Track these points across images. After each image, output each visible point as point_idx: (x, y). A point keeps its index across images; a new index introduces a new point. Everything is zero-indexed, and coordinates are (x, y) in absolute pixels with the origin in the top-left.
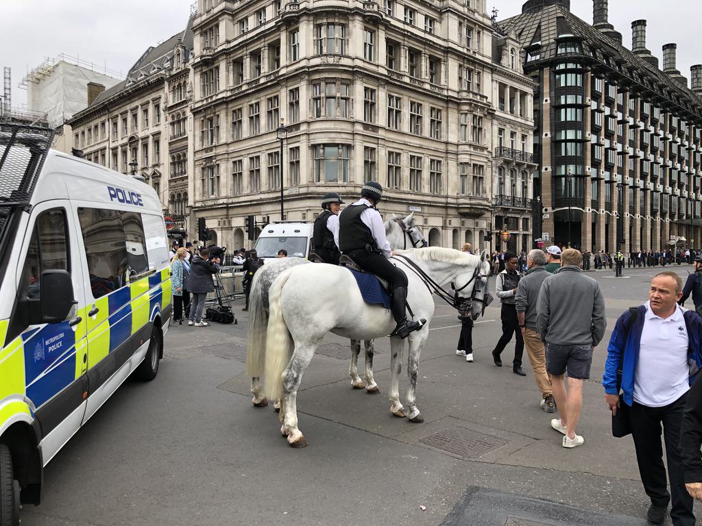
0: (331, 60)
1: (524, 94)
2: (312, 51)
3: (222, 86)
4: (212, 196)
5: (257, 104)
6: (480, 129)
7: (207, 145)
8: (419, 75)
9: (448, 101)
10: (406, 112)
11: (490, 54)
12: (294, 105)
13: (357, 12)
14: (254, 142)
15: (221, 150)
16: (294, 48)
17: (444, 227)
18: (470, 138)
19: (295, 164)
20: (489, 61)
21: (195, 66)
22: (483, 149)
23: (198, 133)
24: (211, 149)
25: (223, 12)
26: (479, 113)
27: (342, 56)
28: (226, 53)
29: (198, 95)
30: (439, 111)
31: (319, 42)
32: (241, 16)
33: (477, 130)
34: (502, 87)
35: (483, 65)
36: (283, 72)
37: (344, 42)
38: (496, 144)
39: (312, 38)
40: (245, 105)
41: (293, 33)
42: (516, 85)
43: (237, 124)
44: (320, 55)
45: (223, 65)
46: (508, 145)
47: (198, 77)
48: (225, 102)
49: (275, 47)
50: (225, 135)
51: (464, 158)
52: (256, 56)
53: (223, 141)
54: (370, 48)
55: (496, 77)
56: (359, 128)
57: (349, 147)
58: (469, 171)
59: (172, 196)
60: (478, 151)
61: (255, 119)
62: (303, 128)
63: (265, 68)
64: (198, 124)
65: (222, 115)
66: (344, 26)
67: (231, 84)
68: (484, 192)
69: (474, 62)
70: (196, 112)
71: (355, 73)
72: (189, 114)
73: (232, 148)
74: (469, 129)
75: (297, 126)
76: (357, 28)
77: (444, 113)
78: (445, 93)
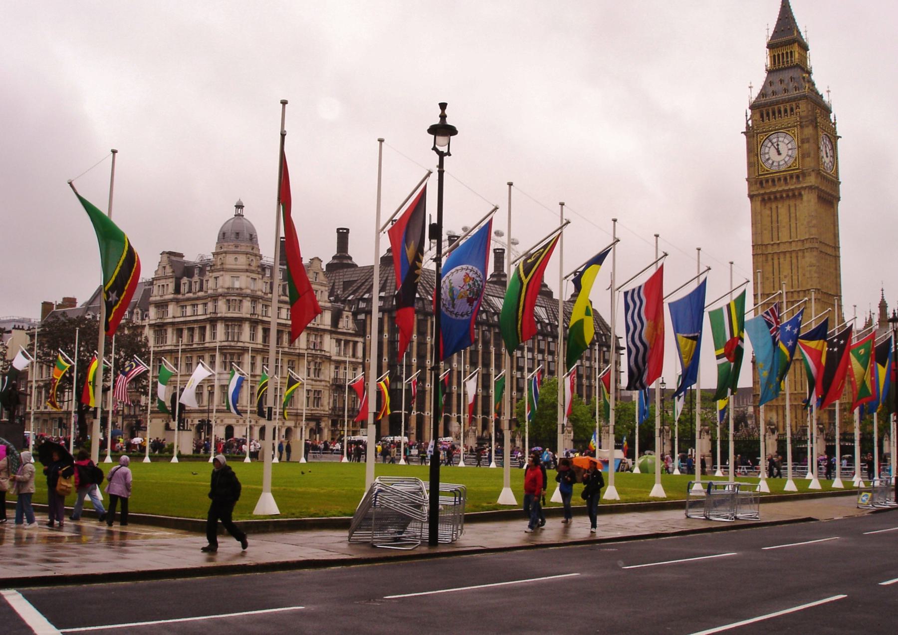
0: (233, 344)
1: (355, 343)
2: (223, 338)
3: (169, 343)
5: (191, 357)
6: (320, 370)
8: (282, 344)
11: (330, 323)
13: (246, 319)
16: (214, 336)
17: (295, 427)
18: (312, 376)
19: (211, 394)
20: (329, 328)
21: (150, 325)
22: (321, 381)
25: (171, 300)
26: (319, 360)
27: (238, 341)
28: (173, 324)
30: (293, 361)
31: (227, 334)
32: (182, 304)
33: (318, 371)
34: (338, 341)
35: (325, 331)
37: (240, 334)
38: (333, 375)
39: (223, 331)
41: (214, 327)
42: (349, 338)
44: (227, 341)
45: (170, 331)
46: (341, 376)
49: (203, 329)
52: (191, 330)
54: (253, 337)
55: (334, 336)
58: (311, 394)
60: (318, 383)
63: (196, 339)
66: (240, 326)
67: (175, 341)
68: (322, 406)
69: (317, 330)
71: (245, 350)
74: (312, 371)
76: (246, 328)
77: (297, 362)
78: (297, 351)
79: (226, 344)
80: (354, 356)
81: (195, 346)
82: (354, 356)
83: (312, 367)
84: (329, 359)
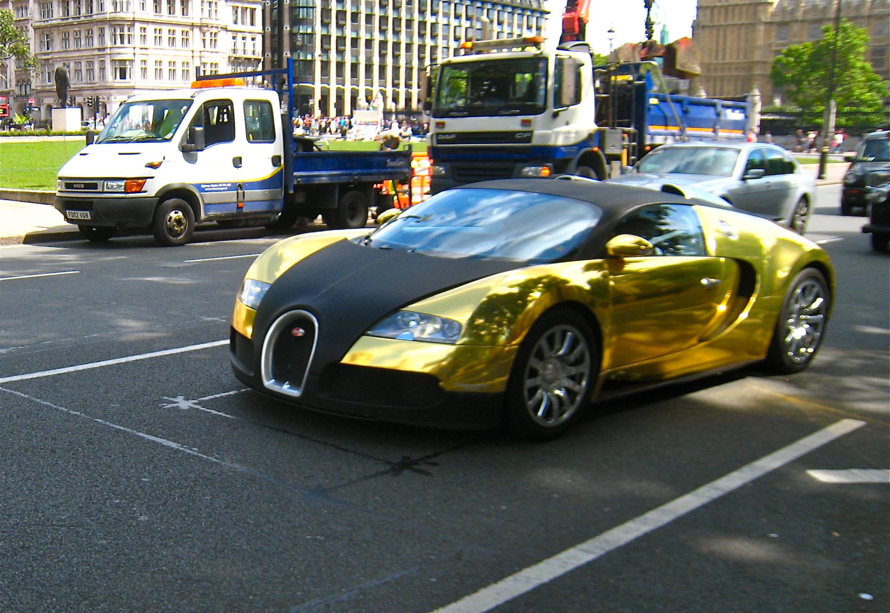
1: (253, 11)
3: (55, 16)
4: (49, 84)
7: (45, 50)
9: (192, 26)
10: (165, 35)
12: (102, 36)
14: (77, 54)
15: (56, 56)
19: (103, 69)
23: (38, 41)
24: (48, 54)
26: (214, 30)
29: (37, 17)
36: (95, 17)
40: (71, 30)
43: (66, 39)
47: (36, 6)
48: (57, 26)
50: (57, 46)
51: (204, 60)
53: (56, 50)
56: (137, 51)
57: (132, 61)
59: (18, 81)
61: (78, 40)
62: (108, 51)
63: (83, 11)
64: (37, 36)
65: (55, 33)
67: (61, 14)
70: (36, 29)
71: (134, 21)
72: (31, 30)
73: (62, 55)
75: (104, 49)
79: (113, 15)
80: (252, 24)
81: (82, 19)
82: (252, 24)
83: (208, 37)
84: (225, 29)
